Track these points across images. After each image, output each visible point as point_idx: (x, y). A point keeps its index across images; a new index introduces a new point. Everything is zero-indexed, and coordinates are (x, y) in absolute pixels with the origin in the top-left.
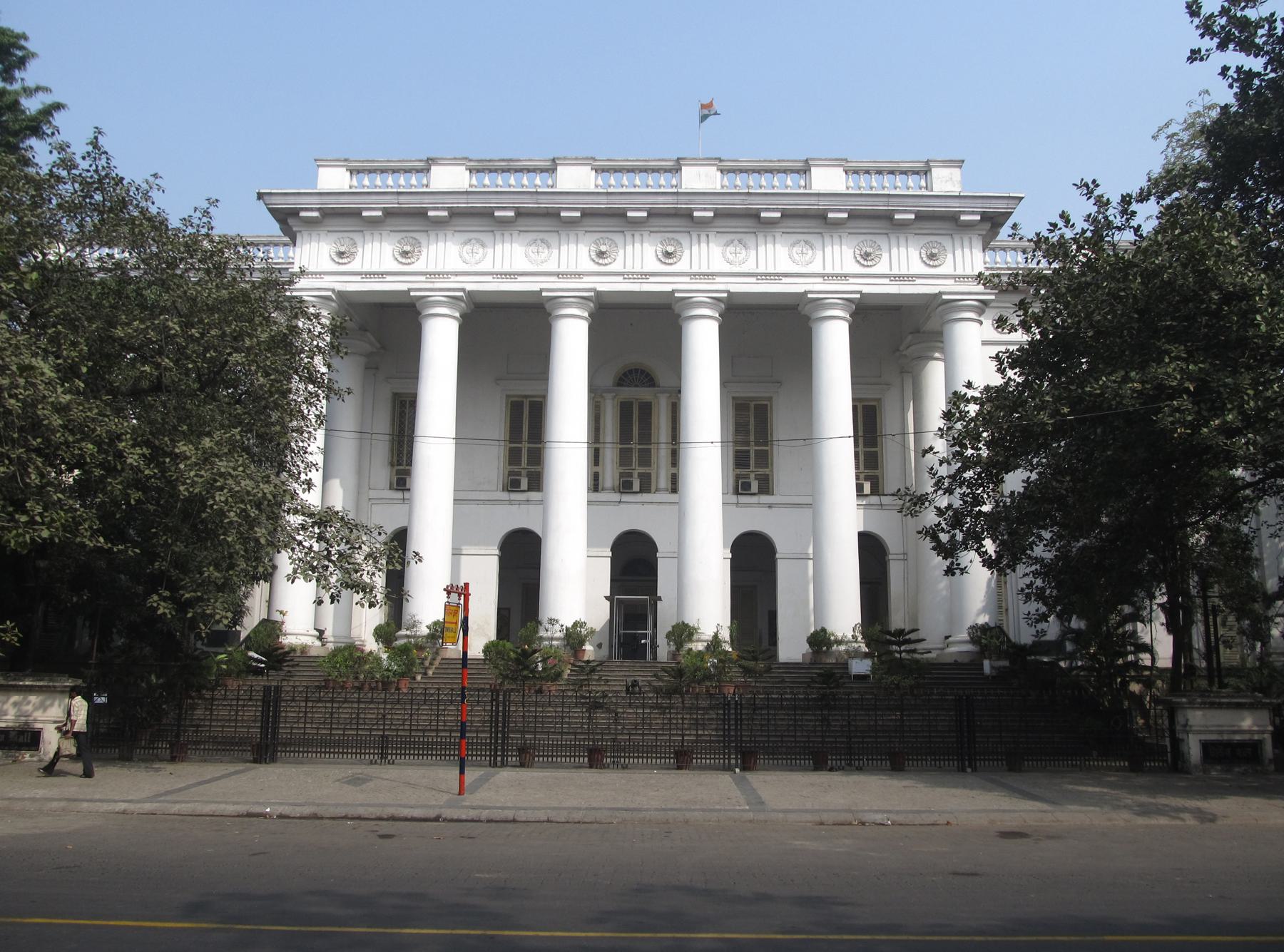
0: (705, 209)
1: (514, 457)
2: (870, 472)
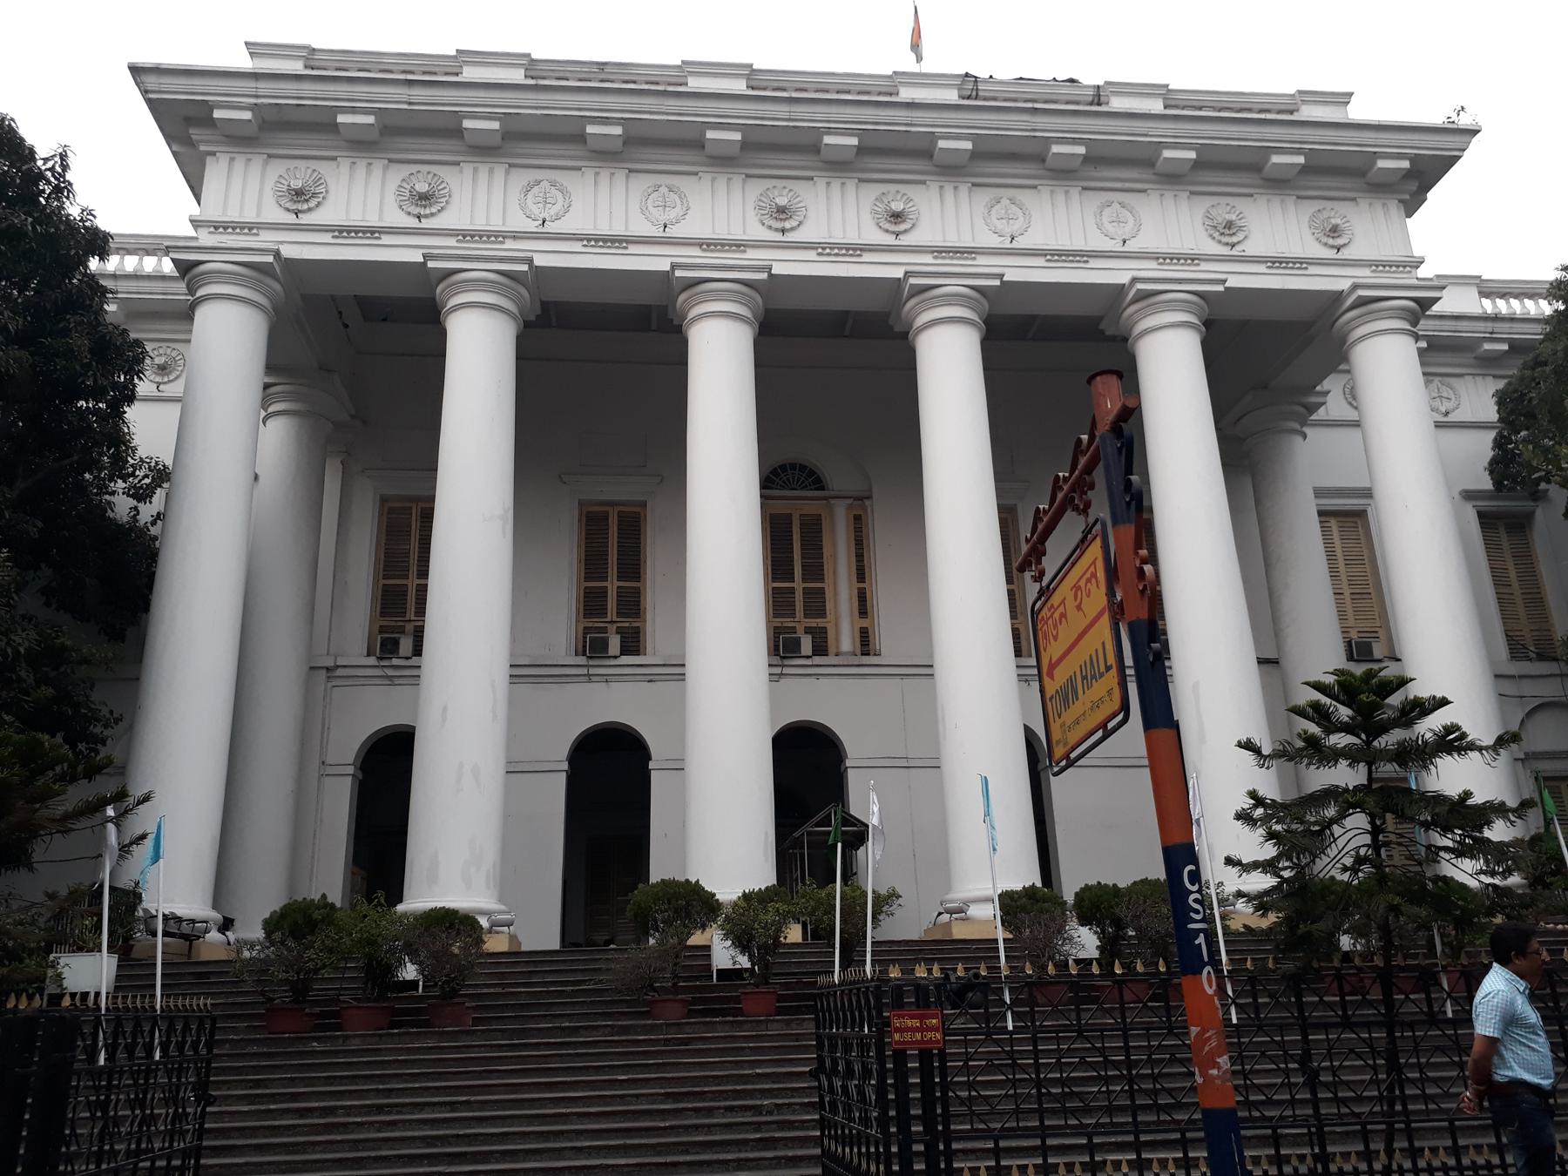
1: (591, 603)
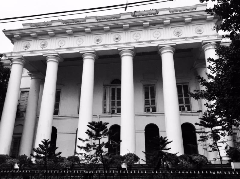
0: (126, 24)
2: (187, 105)
